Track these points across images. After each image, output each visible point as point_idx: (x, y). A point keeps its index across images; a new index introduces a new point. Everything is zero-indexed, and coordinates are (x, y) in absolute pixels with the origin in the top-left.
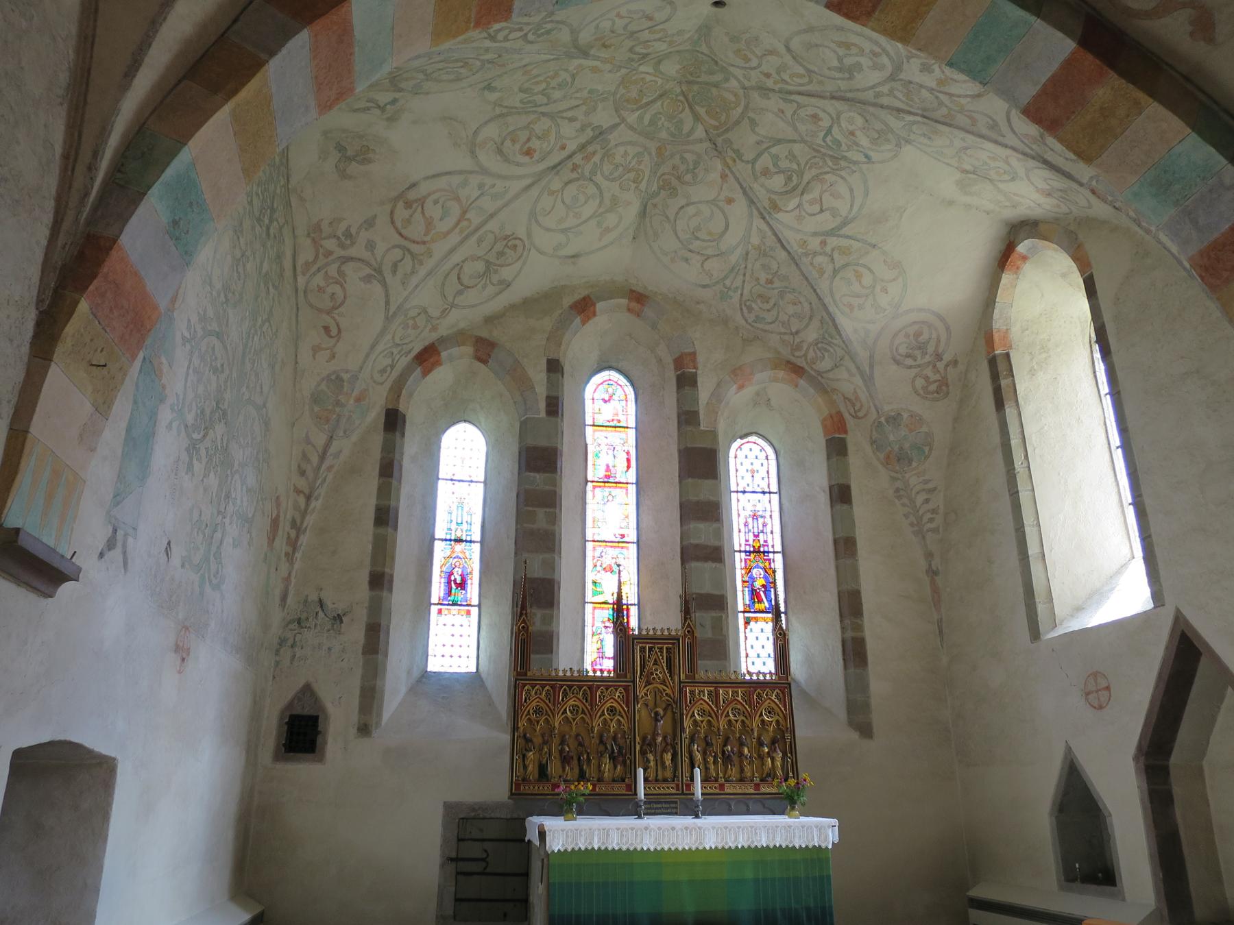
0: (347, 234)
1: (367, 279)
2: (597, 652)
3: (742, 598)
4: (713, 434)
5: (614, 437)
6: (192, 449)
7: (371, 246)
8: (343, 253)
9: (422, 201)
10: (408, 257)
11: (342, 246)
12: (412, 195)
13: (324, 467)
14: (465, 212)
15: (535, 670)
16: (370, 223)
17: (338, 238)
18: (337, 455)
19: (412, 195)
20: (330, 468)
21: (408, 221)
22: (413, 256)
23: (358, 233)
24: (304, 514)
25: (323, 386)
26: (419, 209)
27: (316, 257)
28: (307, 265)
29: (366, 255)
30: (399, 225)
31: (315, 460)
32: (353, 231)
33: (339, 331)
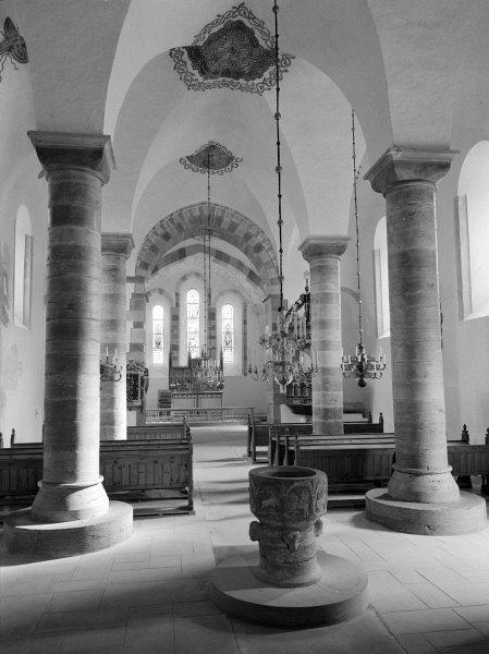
2: (183, 363)
3: (224, 344)
4: (215, 309)
5: (194, 306)
15: (174, 365)
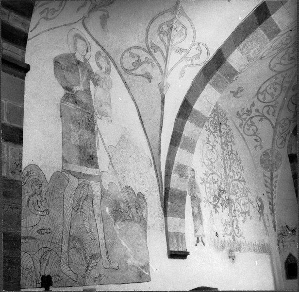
0: (248, 111)
1: (261, 120)
6: (216, 206)
7: (257, 110)
8: (249, 117)
9: (266, 90)
10: (271, 108)
11: (248, 115)
12: (261, 91)
13: (273, 182)
14: (282, 86)
16: (253, 105)
18: (276, 177)
19: (261, 91)
20: (276, 182)
21: (265, 98)
22: (272, 106)
24: (272, 199)
27: (242, 122)
28: (240, 125)
29: (257, 114)
30: (262, 100)
31: (269, 181)
32: (249, 109)
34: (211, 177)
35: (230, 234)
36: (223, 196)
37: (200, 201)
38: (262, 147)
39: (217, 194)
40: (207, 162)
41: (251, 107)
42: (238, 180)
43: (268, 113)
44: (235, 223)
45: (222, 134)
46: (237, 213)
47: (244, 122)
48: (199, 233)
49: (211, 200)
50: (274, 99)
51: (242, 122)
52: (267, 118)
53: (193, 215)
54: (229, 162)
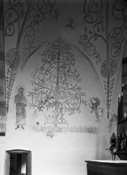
1: (96, 39)
7: (90, 32)
8: (87, 40)
10: (99, 24)
11: (86, 39)
17: (84, 39)
20: (113, 84)
22: (100, 23)
23: (86, 34)
25: (102, 69)
26: (91, 13)
27: (84, 47)
28: (84, 49)
29: (92, 35)
30: (90, 21)
32: (85, 34)
33: (99, 55)
34: (40, 90)
35: (52, 123)
36: (51, 101)
37: (25, 105)
38: (101, 61)
39: (44, 100)
40: (37, 82)
41: (85, 32)
42: (71, 89)
43: (98, 30)
44: (60, 115)
45: (60, 60)
46: (64, 110)
47: (85, 46)
48: (21, 123)
49: (37, 104)
50: (99, 15)
51: (84, 47)
52: (100, 36)
53: (17, 113)
54: (63, 79)
